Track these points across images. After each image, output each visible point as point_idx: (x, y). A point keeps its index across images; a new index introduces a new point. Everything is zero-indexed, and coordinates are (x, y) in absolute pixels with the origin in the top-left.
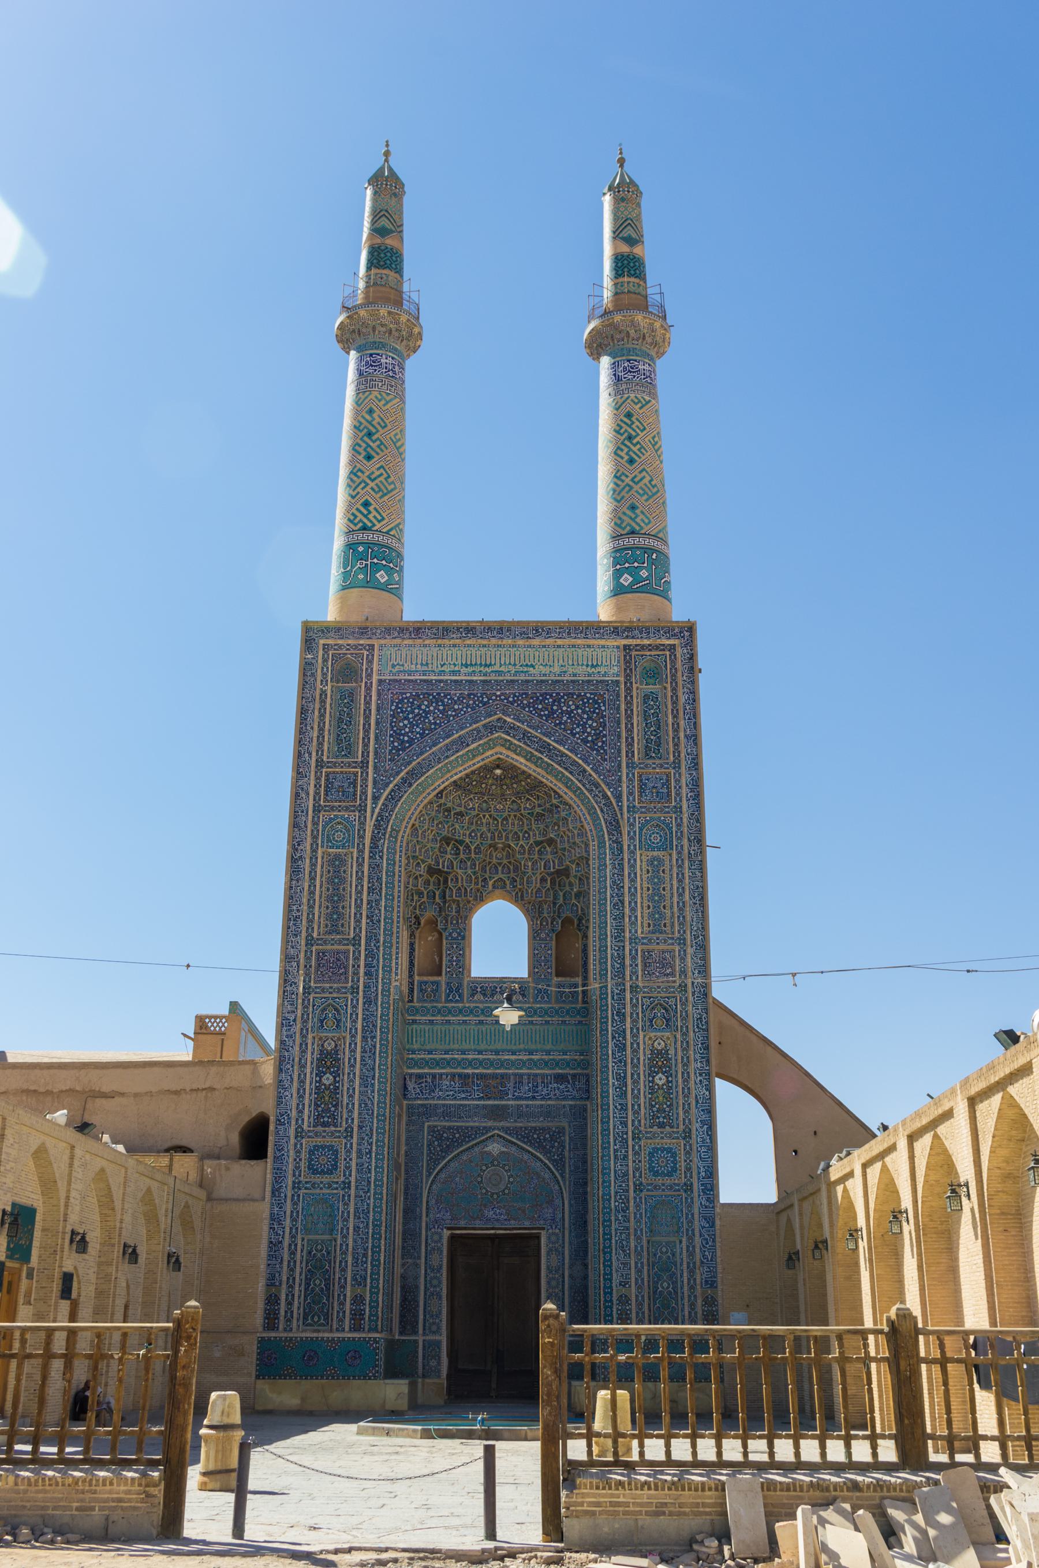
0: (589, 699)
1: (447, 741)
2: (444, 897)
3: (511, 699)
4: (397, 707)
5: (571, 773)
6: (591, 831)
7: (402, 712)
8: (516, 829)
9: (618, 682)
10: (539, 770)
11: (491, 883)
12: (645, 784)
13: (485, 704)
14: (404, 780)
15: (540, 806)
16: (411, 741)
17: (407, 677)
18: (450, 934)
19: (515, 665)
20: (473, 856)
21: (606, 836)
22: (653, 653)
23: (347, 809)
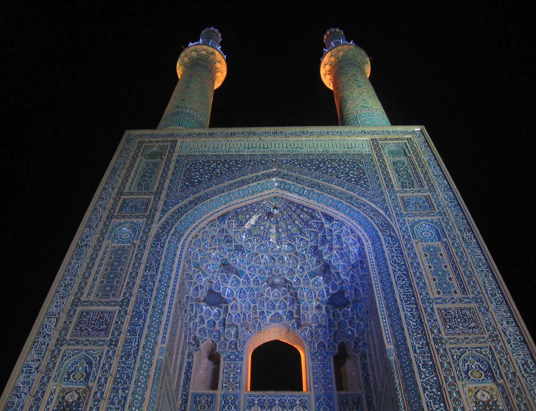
0: (348, 162)
1: (231, 182)
2: (224, 325)
3: (285, 162)
4: (191, 166)
5: (340, 198)
6: (364, 235)
7: (195, 168)
8: (291, 266)
9: (370, 155)
10: (311, 201)
11: (268, 318)
12: (408, 202)
13: (263, 164)
14: (191, 202)
15: (311, 241)
16: (200, 182)
17: (201, 153)
18: (229, 356)
19: (287, 147)
20: (252, 285)
21: (380, 233)
22: (394, 142)
23: (137, 217)
